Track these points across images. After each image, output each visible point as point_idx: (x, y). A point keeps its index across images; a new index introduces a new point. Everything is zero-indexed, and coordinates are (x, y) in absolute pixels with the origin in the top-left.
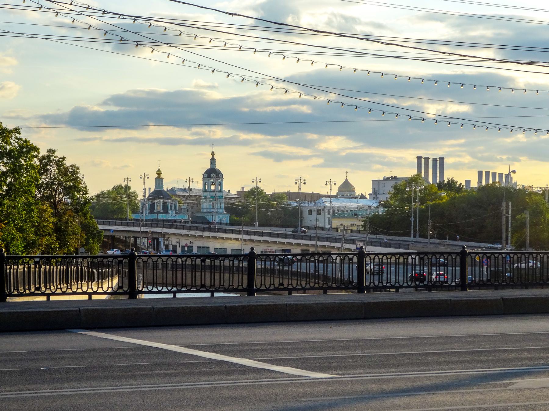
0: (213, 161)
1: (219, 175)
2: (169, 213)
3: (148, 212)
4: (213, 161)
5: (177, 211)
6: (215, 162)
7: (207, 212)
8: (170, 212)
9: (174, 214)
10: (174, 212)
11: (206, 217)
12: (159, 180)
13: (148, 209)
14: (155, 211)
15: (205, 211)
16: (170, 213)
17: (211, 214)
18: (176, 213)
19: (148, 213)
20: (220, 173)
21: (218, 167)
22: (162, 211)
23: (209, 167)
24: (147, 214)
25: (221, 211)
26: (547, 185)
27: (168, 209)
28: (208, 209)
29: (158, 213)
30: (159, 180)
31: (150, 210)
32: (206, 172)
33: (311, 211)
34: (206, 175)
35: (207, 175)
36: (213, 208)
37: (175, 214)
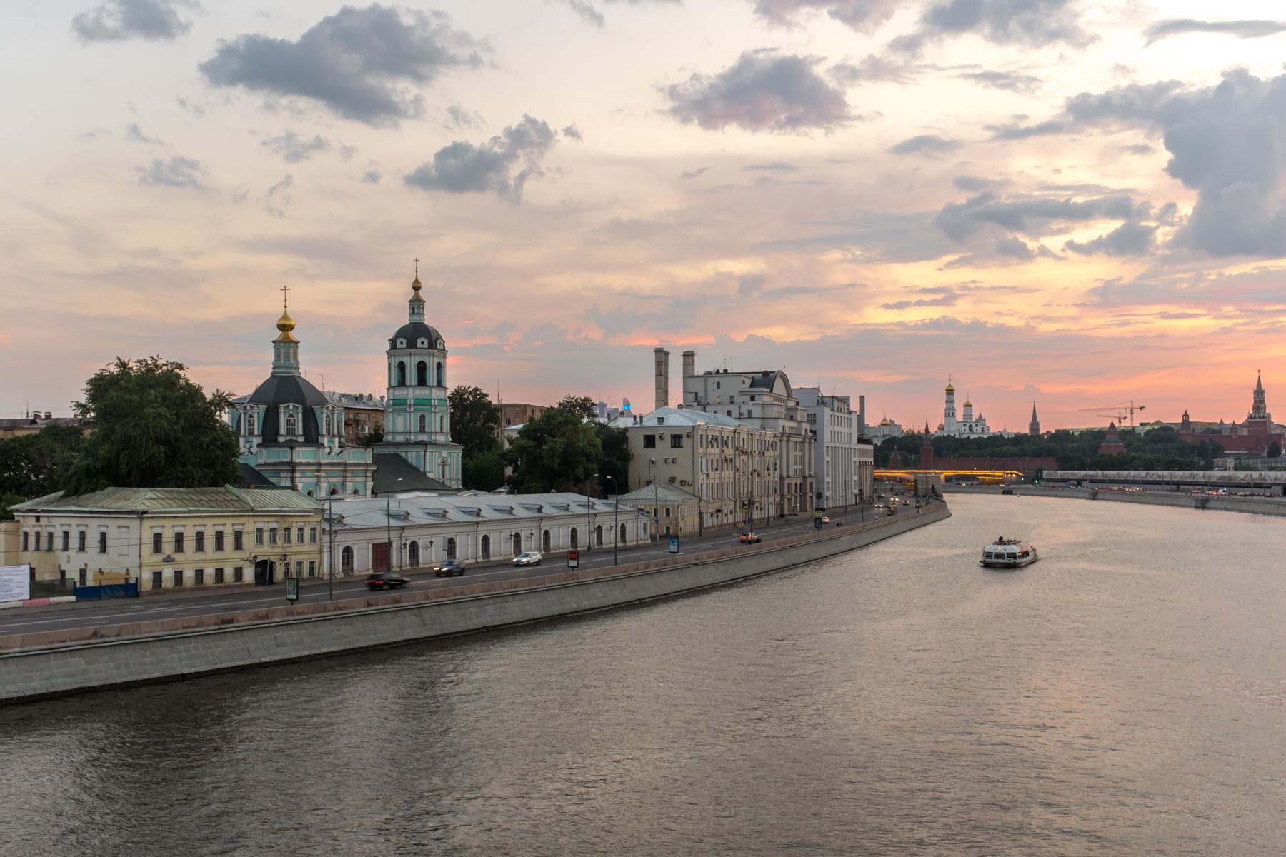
0: (416, 304)
1: (438, 342)
2: (323, 445)
4: (416, 304)
5: (343, 440)
6: (423, 308)
7: (408, 444)
8: (325, 441)
9: (336, 449)
10: (336, 440)
11: (403, 454)
13: (256, 432)
14: (281, 440)
15: (400, 439)
16: (326, 445)
17: (420, 450)
18: (341, 446)
19: (259, 446)
20: (439, 337)
21: (428, 321)
23: (405, 320)
24: (254, 449)
26: (1259, 371)
27: (318, 434)
29: (291, 445)
32: (401, 333)
33: (653, 437)
34: (402, 342)
35: (404, 341)
36: (422, 430)
37: (339, 447)
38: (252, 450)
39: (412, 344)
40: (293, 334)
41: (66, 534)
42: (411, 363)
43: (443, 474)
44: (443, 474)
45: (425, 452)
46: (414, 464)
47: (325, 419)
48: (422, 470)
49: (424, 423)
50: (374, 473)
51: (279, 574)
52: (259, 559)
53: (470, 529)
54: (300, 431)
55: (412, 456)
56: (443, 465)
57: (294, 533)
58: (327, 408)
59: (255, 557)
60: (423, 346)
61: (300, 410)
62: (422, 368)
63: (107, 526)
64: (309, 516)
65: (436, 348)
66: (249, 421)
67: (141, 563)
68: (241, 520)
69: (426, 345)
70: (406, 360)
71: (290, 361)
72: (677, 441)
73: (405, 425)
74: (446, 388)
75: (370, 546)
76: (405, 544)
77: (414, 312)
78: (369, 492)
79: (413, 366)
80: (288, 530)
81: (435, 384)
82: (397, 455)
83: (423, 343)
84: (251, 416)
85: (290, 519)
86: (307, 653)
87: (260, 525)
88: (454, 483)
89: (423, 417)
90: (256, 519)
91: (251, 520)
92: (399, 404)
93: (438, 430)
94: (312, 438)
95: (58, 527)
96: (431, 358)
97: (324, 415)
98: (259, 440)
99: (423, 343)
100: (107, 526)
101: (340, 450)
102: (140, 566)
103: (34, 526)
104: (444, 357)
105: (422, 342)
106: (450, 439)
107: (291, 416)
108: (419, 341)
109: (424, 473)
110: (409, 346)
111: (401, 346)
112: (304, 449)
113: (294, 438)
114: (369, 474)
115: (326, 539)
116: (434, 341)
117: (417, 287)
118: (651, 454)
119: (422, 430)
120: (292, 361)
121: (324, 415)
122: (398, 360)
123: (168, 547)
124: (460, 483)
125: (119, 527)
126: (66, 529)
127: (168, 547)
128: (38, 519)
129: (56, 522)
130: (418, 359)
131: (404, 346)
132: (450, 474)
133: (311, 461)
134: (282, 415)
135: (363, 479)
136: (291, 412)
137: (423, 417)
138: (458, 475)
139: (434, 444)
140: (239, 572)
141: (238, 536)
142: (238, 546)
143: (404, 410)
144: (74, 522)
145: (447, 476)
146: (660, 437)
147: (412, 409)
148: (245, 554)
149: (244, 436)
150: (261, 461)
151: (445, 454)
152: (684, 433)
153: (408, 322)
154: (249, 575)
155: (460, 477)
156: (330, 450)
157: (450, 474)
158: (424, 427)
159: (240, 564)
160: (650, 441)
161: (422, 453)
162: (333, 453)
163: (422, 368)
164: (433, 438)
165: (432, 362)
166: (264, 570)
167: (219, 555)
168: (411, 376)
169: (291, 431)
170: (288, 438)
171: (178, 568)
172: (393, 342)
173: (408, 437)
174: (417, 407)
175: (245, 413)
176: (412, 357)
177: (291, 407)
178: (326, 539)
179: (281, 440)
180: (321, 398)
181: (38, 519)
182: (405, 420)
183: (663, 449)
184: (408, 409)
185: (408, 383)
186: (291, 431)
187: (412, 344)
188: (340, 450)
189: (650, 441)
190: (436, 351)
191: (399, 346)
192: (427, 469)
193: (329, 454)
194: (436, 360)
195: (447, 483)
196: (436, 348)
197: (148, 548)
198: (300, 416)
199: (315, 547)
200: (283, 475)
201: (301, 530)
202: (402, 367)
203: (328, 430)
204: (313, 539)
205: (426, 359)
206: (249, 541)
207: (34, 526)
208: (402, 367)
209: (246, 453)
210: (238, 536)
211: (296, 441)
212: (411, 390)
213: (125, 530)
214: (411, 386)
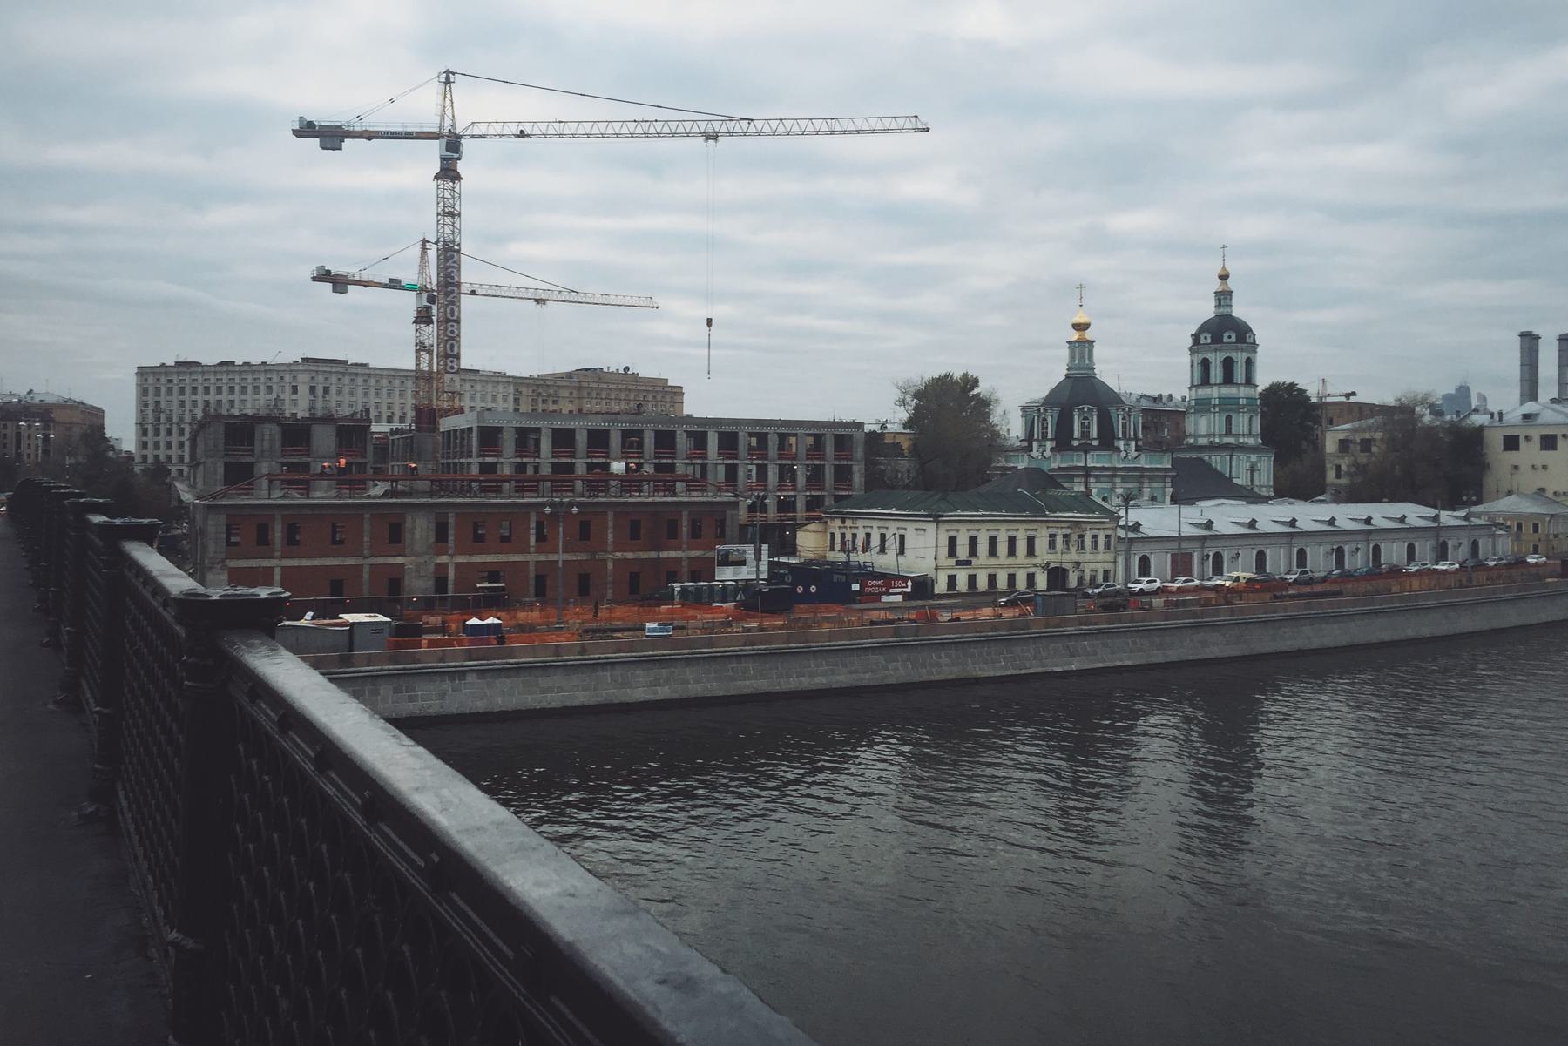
0: (1223, 297)
1: (1248, 335)
2: (1118, 449)
3: (1049, 444)
4: (1223, 297)
5: (1140, 443)
6: (1231, 300)
7: (1213, 448)
8: (1121, 444)
10: (1133, 443)
11: (1206, 458)
12: (1082, 348)
13: (1049, 437)
15: (1203, 441)
19: (1052, 449)
21: (1239, 311)
22: (1095, 443)
23: (1208, 310)
24: (1048, 453)
25: (1251, 441)
27: (1114, 437)
28: (1214, 435)
29: (1086, 449)
30: (1082, 348)
31: (1056, 438)
32: (1205, 327)
34: (1206, 339)
35: (1209, 336)
36: (1228, 432)
37: (1136, 451)
38: (1045, 454)
39: (1217, 339)
40: (1089, 335)
41: (868, 535)
42: (1216, 359)
43: (1252, 480)
44: (1252, 480)
45: (1231, 456)
46: (1219, 468)
47: (1120, 421)
48: (1227, 475)
49: (1231, 424)
50: (1173, 478)
51: (1073, 581)
52: (1052, 565)
53: (1284, 540)
54: (1094, 433)
55: (1217, 461)
56: (1252, 470)
57: (1088, 541)
58: (1123, 410)
59: (1048, 564)
60: (1230, 340)
61: (1095, 413)
62: (1228, 364)
63: (905, 529)
64: (1104, 523)
65: (1245, 342)
66: (1043, 424)
67: (937, 566)
68: (1034, 526)
69: (1234, 339)
70: (1211, 356)
71: (1085, 361)
72: (1549, 442)
73: (1209, 427)
74: (1257, 386)
75: (1169, 555)
76: (1208, 556)
77: (1220, 303)
78: (1168, 499)
79: (1218, 362)
80: (1081, 537)
81: (1244, 382)
82: (1201, 460)
83: (1230, 337)
84: (1045, 419)
85: (1084, 526)
86: (1100, 665)
87: (1052, 531)
88: (1264, 489)
89: (1229, 419)
90: (1050, 525)
91: (1044, 525)
92: (1202, 406)
93: (1246, 431)
94: (1107, 441)
95: (861, 529)
96: (1240, 353)
97: (1120, 417)
98: (1054, 444)
99: (1230, 337)
100: (905, 529)
101: (1136, 454)
102: (937, 568)
103: (840, 527)
104: (1255, 352)
105: (1229, 337)
106: (1261, 441)
107: (1086, 418)
108: (1226, 336)
109: (1231, 478)
110: (1212, 342)
111: (1205, 342)
112: (1098, 453)
113: (1089, 442)
114: (1168, 480)
115: (1122, 547)
116: (1243, 333)
117: (1224, 277)
118: (1512, 457)
119: (1228, 432)
120: (1087, 362)
121: (1120, 417)
122: (1201, 357)
123: (963, 552)
124: (1272, 489)
125: (917, 529)
126: (868, 530)
127: (963, 552)
128: (843, 522)
129: (860, 523)
130: (1224, 355)
131: (1209, 341)
132: (1260, 481)
133: (1106, 465)
134: (1076, 417)
135: (1161, 485)
136: (1085, 415)
137: (1229, 419)
138: (1268, 480)
139: (1241, 447)
140: (1031, 578)
141: (1031, 541)
142: (1031, 552)
143: (1209, 411)
144: (875, 524)
145: (1256, 482)
146: (1526, 437)
147: (1217, 410)
148: (1037, 561)
149: (1038, 440)
150: (1054, 466)
151: (1254, 458)
152: (1559, 432)
153: (1213, 316)
154: (1041, 582)
155: (1271, 483)
156: (1127, 454)
157: (1260, 481)
158: (1231, 428)
159: (1031, 570)
160: (1511, 443)
161: (1228, 457)
162: (1130, 458)
163: (1228, 364)
164: (1241, 440)
165: (1240, 358)
166: (1057, 575)
167: (1011, 561)
168: (1216, 374)
169: (1085, 434)
170: (1083, 442)
171: (971, 572)
172: (1196, 337)
173: (1212, 439)
174: (1223, 407)
175: (1039, 417)
176: (1218, 353)
177: (1086, 409)
178: (1122, 547)
179: (1076, 443)
180: (1115, 398)
181: (843, 522)
182: (1209, 420)
183: (1530, 453)
184: (1212, 409)
185: (1212, 381)
186: (1085, 434)
187: (1217, 339)
188: (1136, 454)
189: (1511, 443)
190: (1245, 345)
191: (1202, 341)
192: (1234, 475)
193: (1125, 458)
194: (1245, 355)
195: (1256, 490)
196: (1245, 342)
197: (944, 551)
198: (1095, 418)
199: (1109, 557)
200: (1076, 480)
201: (1095, 537)
202: (1205, 364)
203: (1124, 433)
204: (1107, 546)
205: (1234, 355)
206: (1041, 544)
207: (840, 527)
208: (1205, 364)
209: (1040, 458)
210: (1031, 541)
211: (1091, 444)
212: (1215, 388)
213: (922, 532)
214: (1215, 384)
